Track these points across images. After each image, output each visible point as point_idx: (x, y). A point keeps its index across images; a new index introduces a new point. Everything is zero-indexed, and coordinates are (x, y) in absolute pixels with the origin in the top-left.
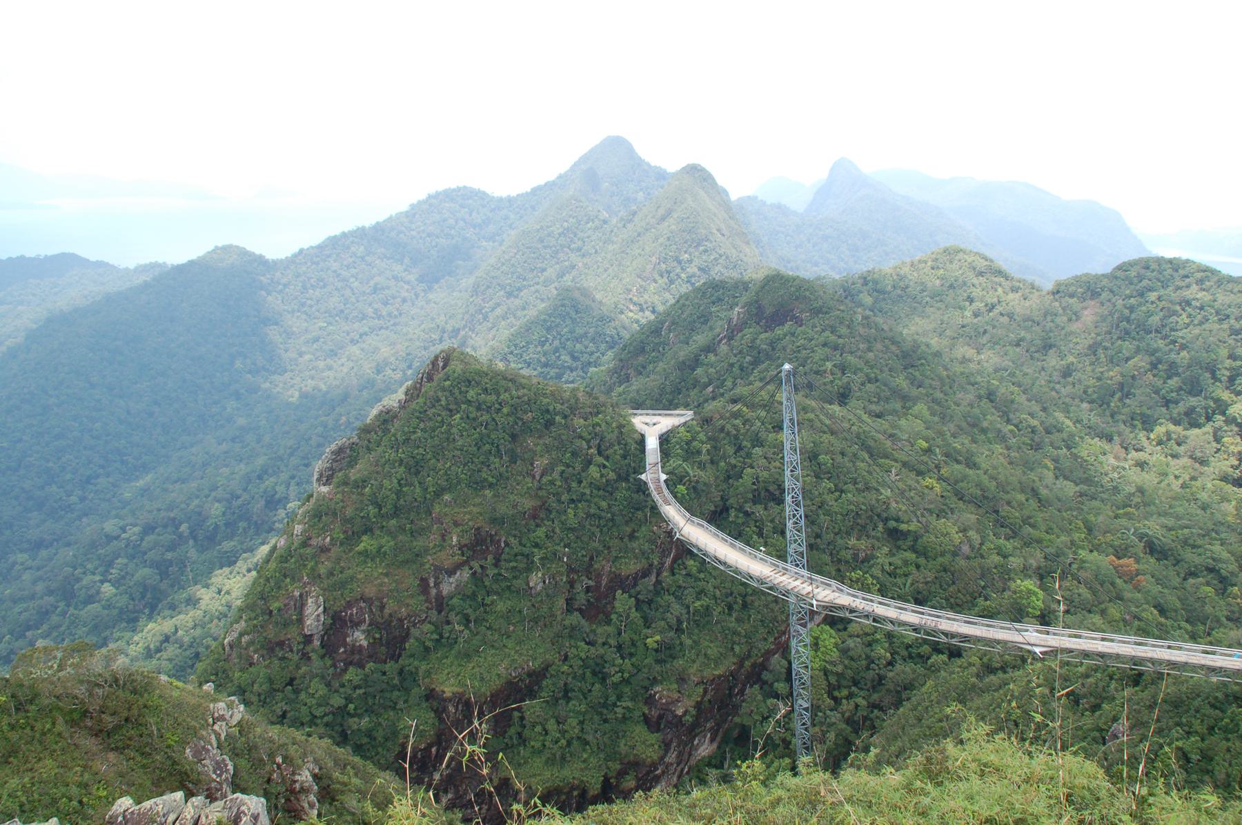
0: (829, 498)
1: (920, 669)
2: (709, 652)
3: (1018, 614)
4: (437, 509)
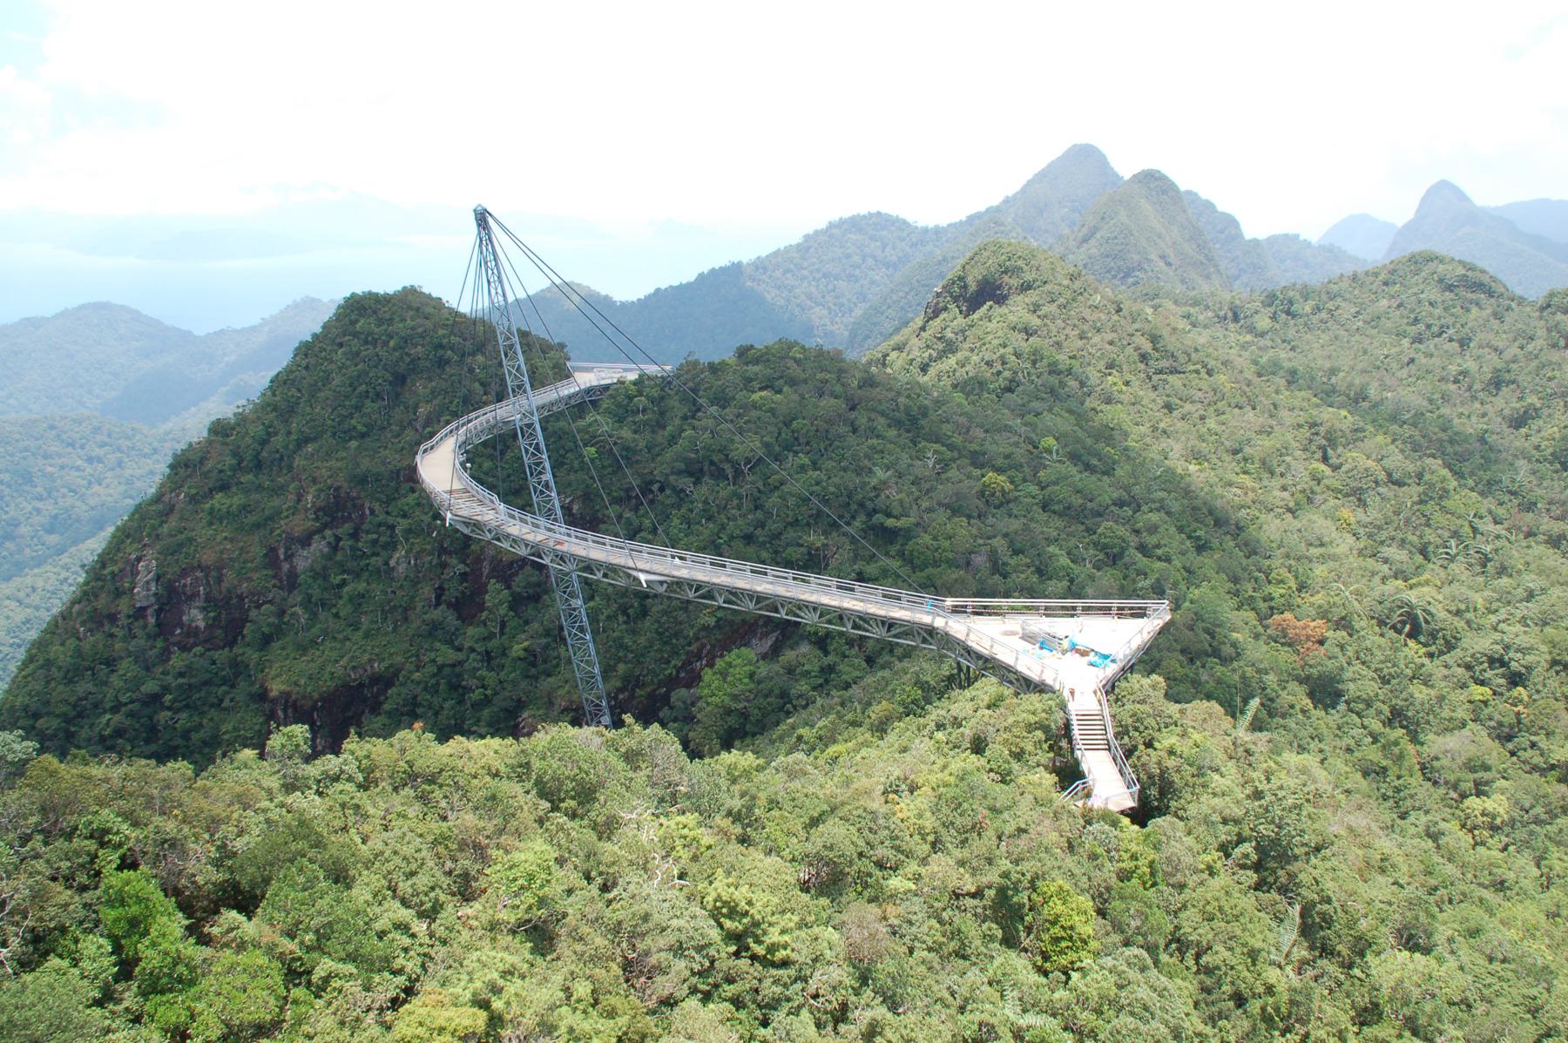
4: (298, 462)
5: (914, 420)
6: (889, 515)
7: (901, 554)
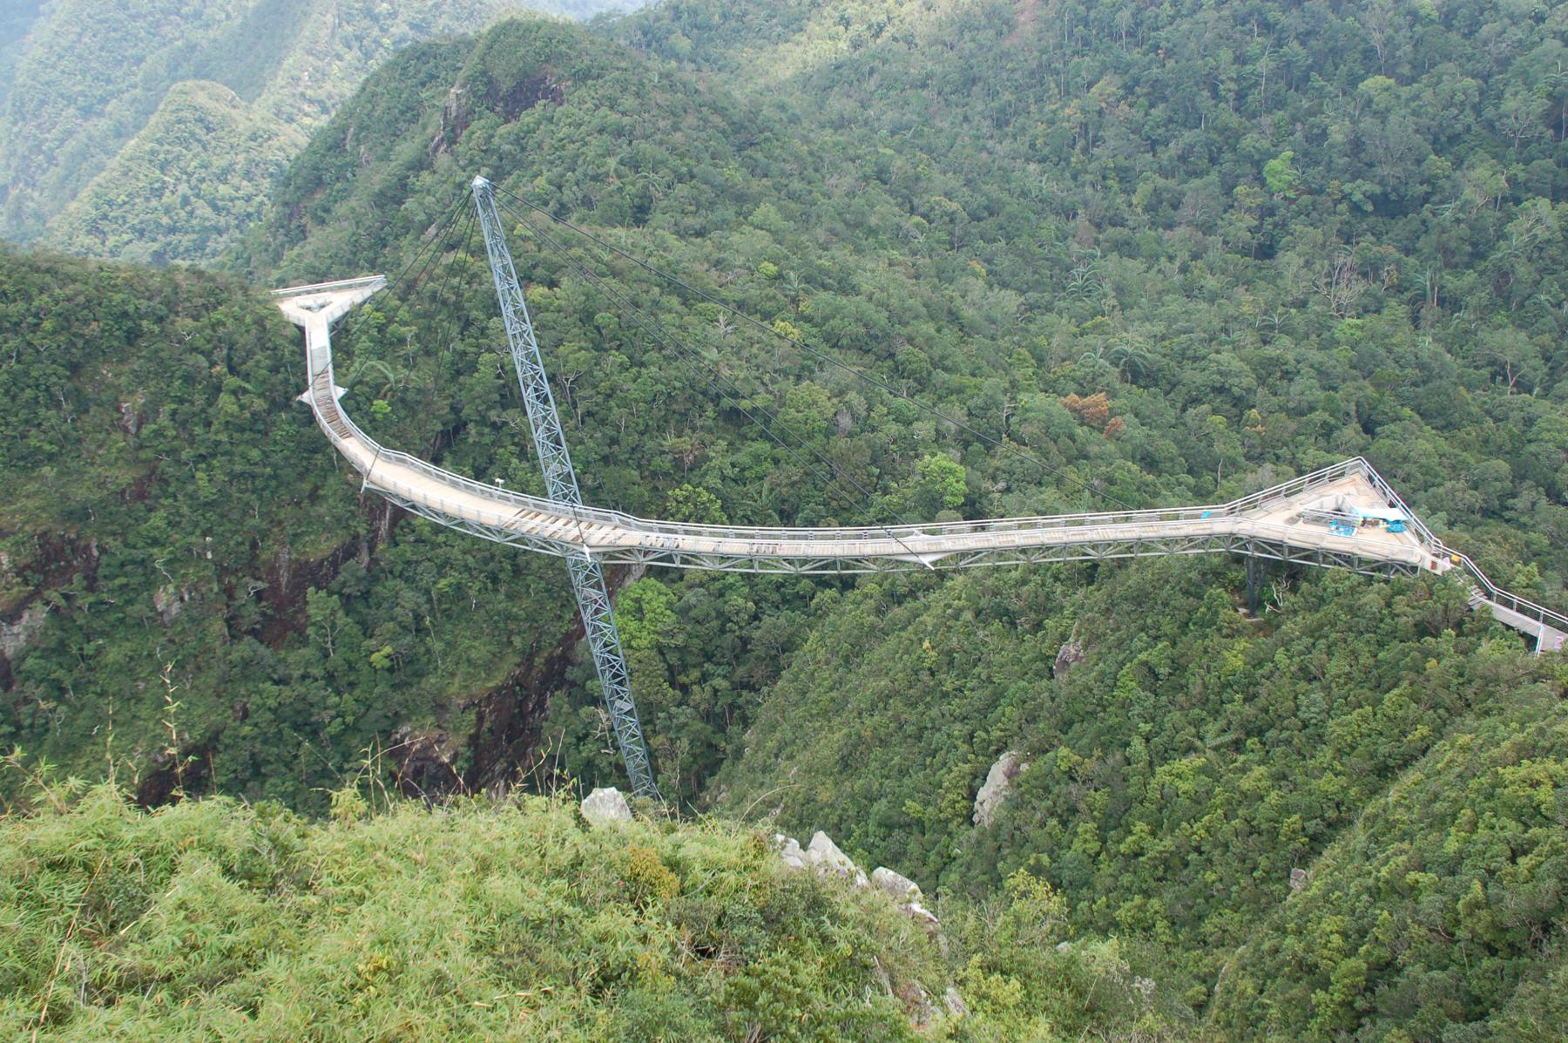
0: (624, 380)
1: (800, 618)
2: (474, 654)
3: (930, 508)
7: (764, 436)
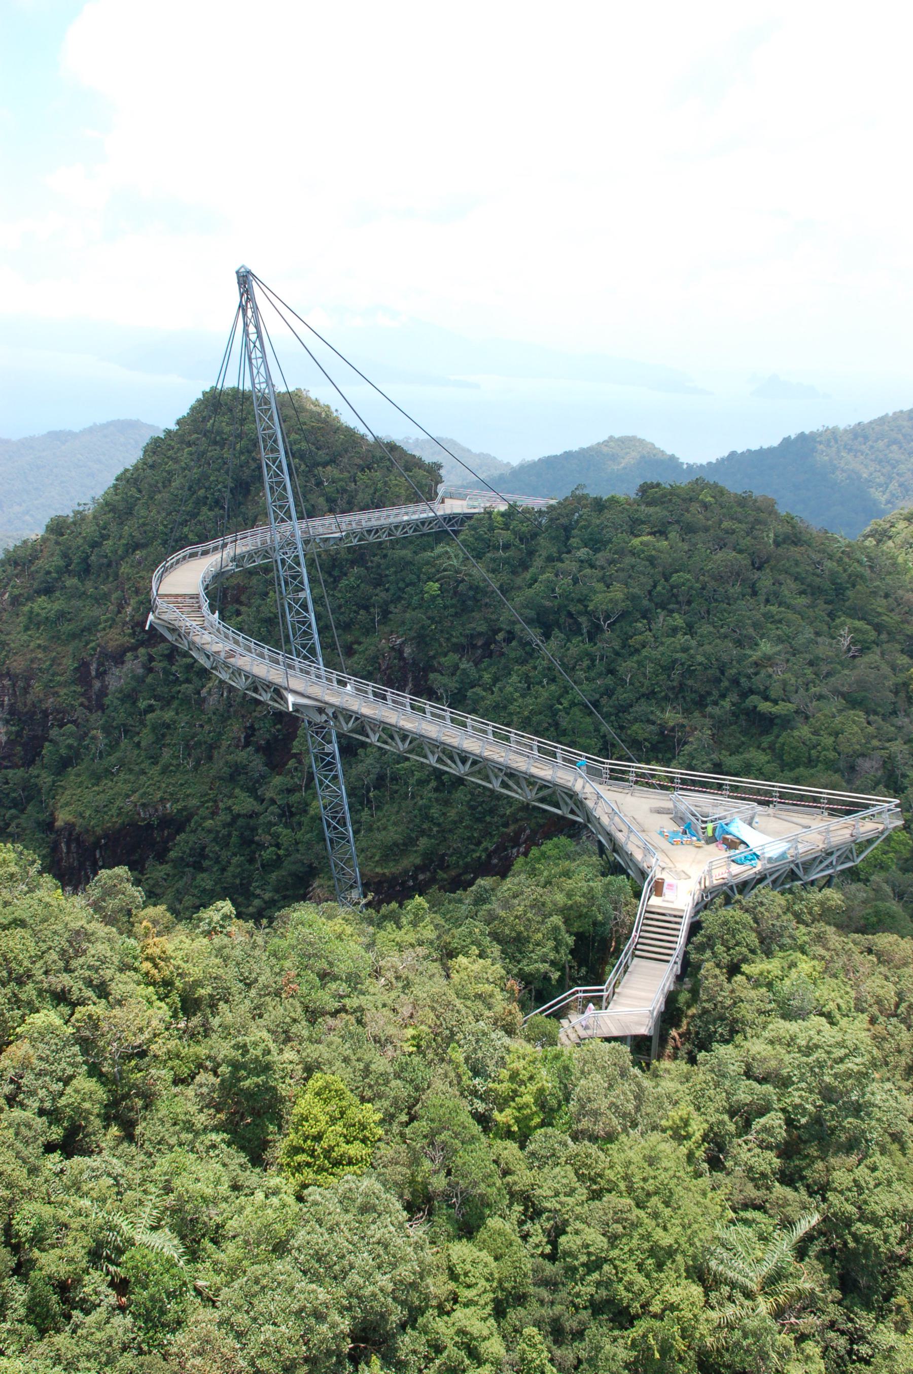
4: (124, 569)
5: (840, 590)
6: (766, 698)
7: (771, 747)
